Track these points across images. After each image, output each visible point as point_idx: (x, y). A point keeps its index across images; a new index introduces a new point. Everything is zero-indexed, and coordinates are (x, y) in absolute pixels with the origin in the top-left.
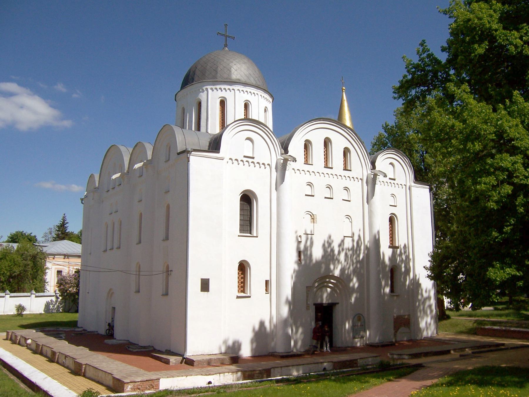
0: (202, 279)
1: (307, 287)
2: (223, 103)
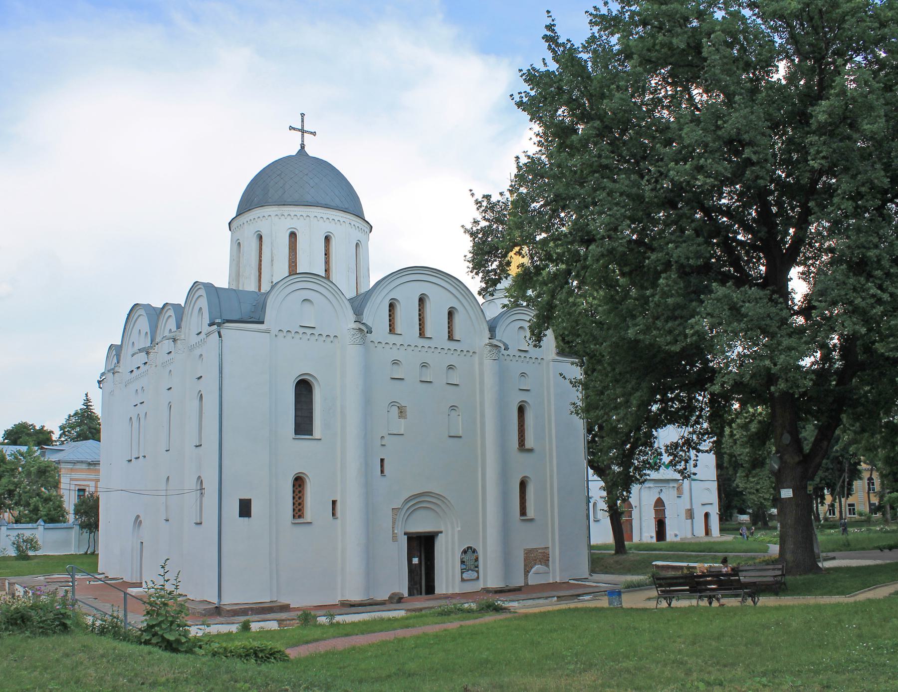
2: (293, 235)
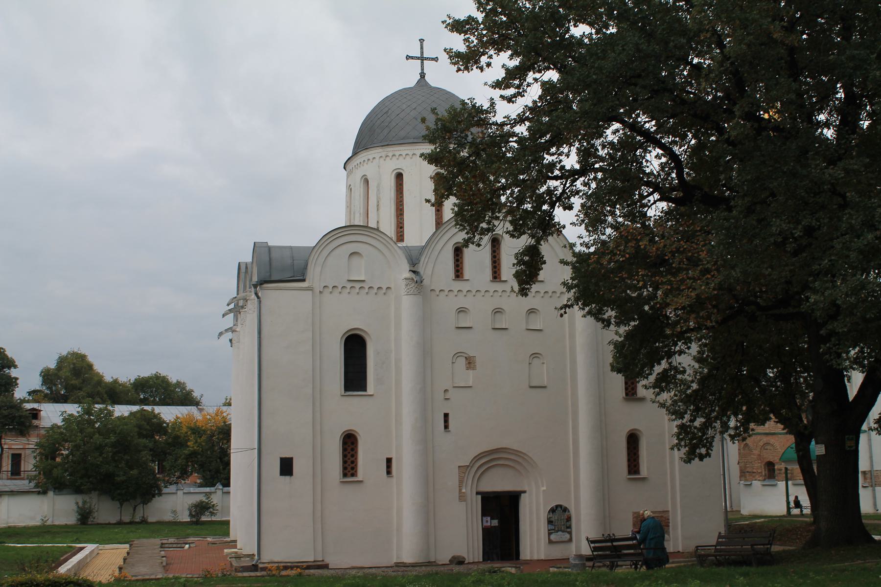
0: (281, 459)
1: (459, 467)
2: (399, 177)
